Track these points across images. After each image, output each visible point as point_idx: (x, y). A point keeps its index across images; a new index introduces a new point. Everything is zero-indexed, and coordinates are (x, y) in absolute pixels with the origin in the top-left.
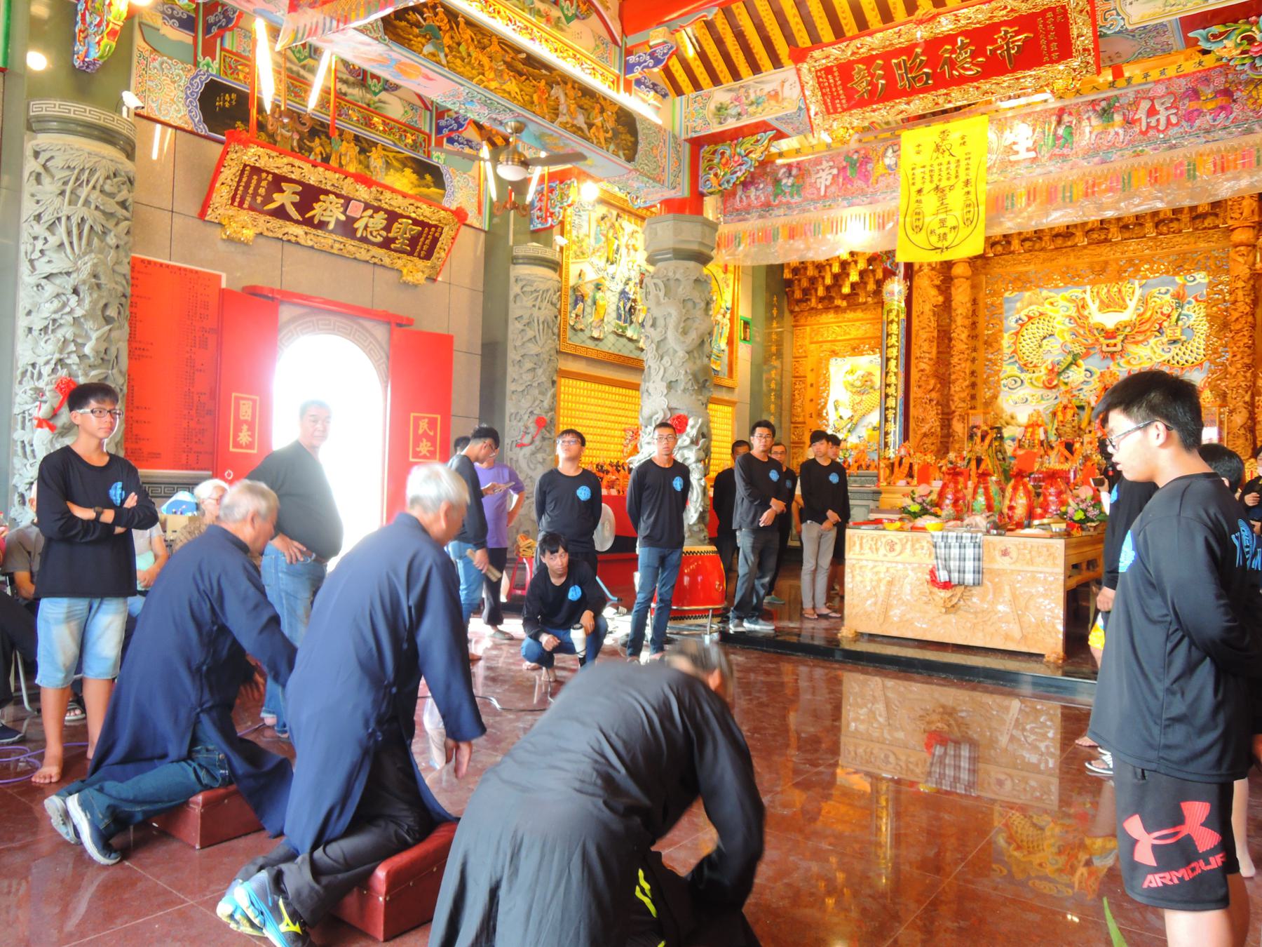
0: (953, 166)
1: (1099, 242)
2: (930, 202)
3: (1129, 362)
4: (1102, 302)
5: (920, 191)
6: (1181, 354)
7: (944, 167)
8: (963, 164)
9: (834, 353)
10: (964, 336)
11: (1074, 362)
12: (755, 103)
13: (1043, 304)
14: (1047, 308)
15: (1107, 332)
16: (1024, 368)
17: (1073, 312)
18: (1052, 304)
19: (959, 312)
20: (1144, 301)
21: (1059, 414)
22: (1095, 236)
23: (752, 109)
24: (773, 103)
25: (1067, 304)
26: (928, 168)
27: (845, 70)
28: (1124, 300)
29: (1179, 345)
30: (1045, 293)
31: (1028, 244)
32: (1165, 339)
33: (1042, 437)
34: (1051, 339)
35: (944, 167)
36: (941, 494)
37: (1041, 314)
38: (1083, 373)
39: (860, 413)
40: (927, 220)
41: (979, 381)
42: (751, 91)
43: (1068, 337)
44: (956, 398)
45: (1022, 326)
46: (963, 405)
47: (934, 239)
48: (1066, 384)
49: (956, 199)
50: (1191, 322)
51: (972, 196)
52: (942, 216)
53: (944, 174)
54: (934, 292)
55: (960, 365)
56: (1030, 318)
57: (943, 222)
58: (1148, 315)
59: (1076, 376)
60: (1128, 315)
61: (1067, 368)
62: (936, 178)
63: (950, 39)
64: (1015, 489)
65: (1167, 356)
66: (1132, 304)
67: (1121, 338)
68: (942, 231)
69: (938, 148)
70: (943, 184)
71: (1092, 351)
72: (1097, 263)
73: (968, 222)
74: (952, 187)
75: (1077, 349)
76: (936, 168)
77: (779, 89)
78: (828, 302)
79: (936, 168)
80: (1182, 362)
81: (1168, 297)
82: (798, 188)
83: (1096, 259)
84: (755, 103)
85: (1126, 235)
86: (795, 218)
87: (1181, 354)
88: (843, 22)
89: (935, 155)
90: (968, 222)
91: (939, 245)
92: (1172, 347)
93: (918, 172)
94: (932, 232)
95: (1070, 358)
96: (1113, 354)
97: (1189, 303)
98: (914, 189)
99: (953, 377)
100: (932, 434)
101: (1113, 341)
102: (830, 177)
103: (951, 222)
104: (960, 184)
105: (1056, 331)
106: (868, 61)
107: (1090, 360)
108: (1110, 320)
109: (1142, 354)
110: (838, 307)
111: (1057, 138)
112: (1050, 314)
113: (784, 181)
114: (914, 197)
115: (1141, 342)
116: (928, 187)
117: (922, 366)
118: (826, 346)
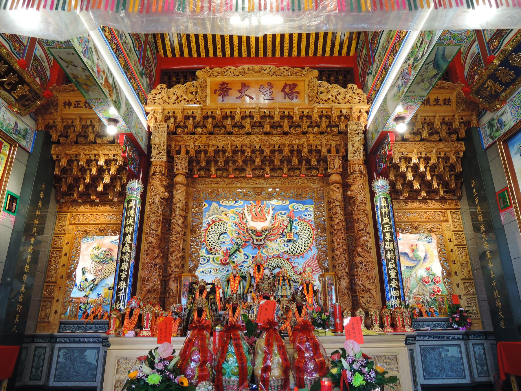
1: (259, 177)
4: (253, 216)
6: (293, 248)
9: (86, 233)
10: (180, 222)
11: (238, 250)
13: (221, 215)
14: (223, 217)
15: (257, 232)
16: (209, 251)
17: (237, 220)
18: (226, 214)
19: (178, 205)
20: (274, 218)
21: (231, 280)
22: (257, 172)
28: (264, 216)
29: (292, 243)
31: (219, 172)
32: (286, 239)
33: (221, 295)
34: (225, 235)
36: (185, 355)
37: (220, 220)
38: (243, 256)
39: (100, 277)
41: (187, 256)
43: (235, 235)
44: (172, 265)
45: (209, 226)
46: (177, 270)
48: (234, 262)
50: (297, 231)
54: (162, 189)
55: (176, 240)
56: (214, 222)
58: (276, 225)
59: (240, 257)
60: (267, 224)
61: (235, 252)
64: (269, 345)
65: (287, 249)
66: (269, 218)
67: (264, 236)
71: (248, 244)
72: (258, 188)
75: (239, 242)
78: (86, 198)
80: (294, 252)
81: (285, 216)
83: (256, 186)
85: (273, 174)
87: (293, 248)
92: (289, 244)
96: (259, 245)
97: (296, 220)
99: (171, 250)
100: (155, 290)
101: (260, 238)
105: (228, 231)
107: (246, 249)
108: (259, 226)
109: (274, 247)
110: (93, 201)
112: (225, 220)
115: (273, 240)
117: (150, 239)
118: (82, 227)
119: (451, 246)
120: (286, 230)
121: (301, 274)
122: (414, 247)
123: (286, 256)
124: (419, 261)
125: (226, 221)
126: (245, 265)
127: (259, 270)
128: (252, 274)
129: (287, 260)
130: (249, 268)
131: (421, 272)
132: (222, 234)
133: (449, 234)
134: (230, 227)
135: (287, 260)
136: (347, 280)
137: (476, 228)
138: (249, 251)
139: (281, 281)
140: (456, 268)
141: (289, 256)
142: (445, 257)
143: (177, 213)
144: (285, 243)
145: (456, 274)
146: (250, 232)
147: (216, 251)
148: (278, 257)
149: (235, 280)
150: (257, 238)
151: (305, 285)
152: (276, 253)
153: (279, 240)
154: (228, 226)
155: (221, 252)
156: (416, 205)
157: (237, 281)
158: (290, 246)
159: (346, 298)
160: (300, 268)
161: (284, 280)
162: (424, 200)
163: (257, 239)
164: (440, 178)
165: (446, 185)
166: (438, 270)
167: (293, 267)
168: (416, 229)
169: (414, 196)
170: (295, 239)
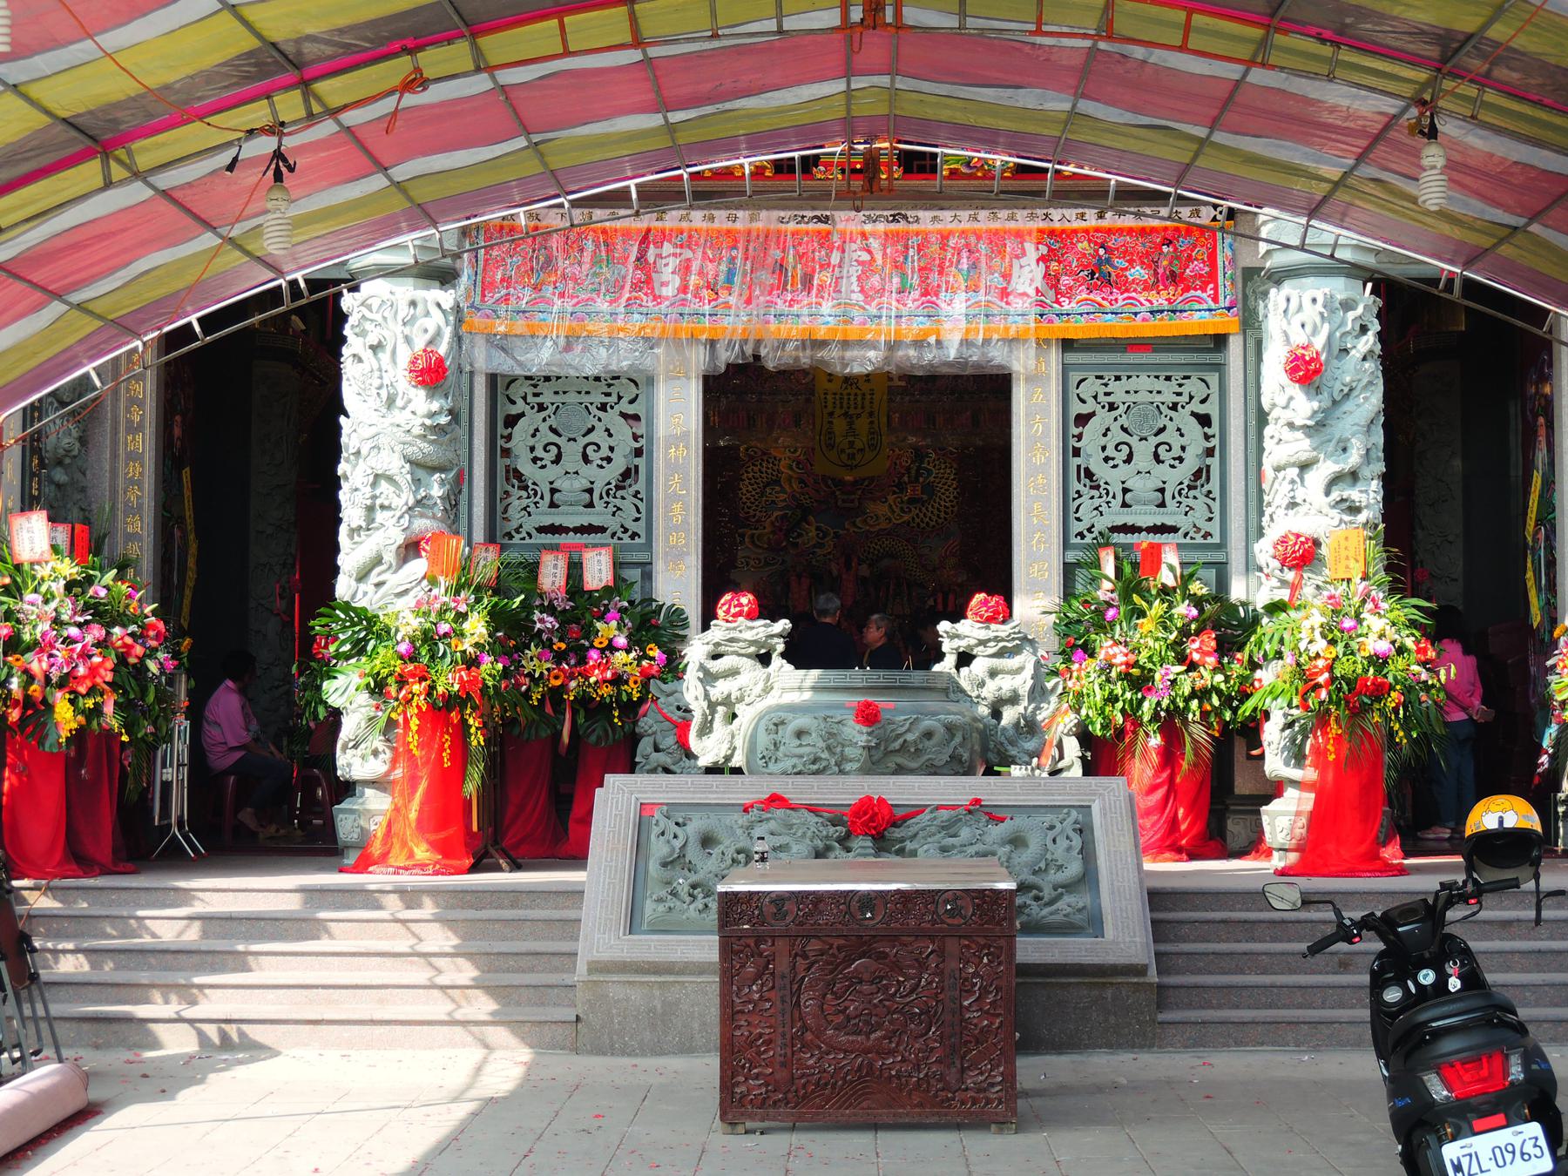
2: (840, 425)
3: (865, 521)
5: (831, 414)
47: (844, 457)
49: (862, 424)
65: (906, 518)
70: (852, 411)
73: (872, 447)
74: (859, 416)
90: (872, 447)
94: (843, 451)
98: (826, 411)
103: (859, 444)
116: (838, 412)
120: (906, 479)
125: (779, 456)
128: (835, 573)
132: (768, 484)
151: (940, 595)
170: (925, 497)
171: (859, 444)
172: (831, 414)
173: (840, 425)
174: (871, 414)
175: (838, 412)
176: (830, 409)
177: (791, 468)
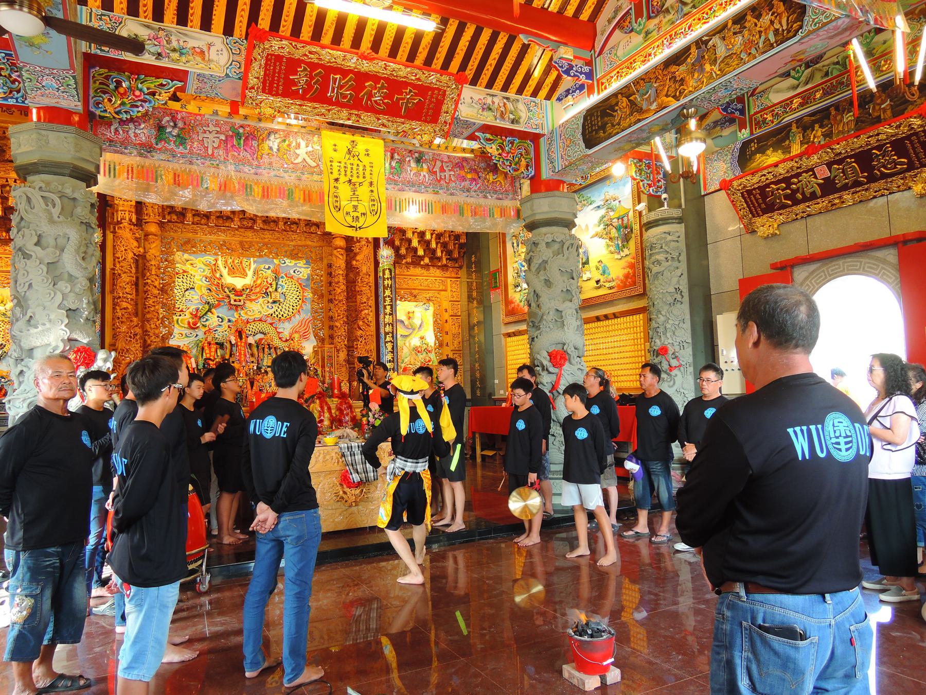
0: (361, 168)
1: (247, 228)
2: (344, 191)
5: (337, 180)
7: (355, 167)
8: (368, 168)
12: (180, 51)
13: (185, 265)
14: (188, 267)
17: (208, 273)
19: (153, 263)
20: (256, 273)
22: (245, 223)
23: (175, 56)
24: (199, 59)
25: (204, 267)
26: (342, 165)
27: (293, 64)
30: (186, 256)
31: (196, 219)
32: (271, 301)
34: (192, 292)
35: (355, 167)
37: (184, 271)
40: (343, 203)
42: (173, 38)
43: (205, 291)
47: (349, 219)
51: (375, 194)
52: (356, 203)
53: (355, 172)
57: (355, 207)
58: (259, 282)
59: (212, 320)
60: (248, 281)
62: (348, 173)
63: (375, 78)
65: (271, 311)
66: (250, 273)
68: (355, 214)
69: (349, 152)
70: (354, 180)
75: (211, 301)
76: (349, 166)
77: (205, 49)
79: (349, 166)
81: (269, 271)
82: (182, 140)
84: (180, 51)
85: (265, 227)
86: (178, 165)
88: (283, 23)
89: (348, 156)
91: (354, 224)
93: (335, 164)
95: (207, 307)
96: (237, 306)
102: (217, 141)
103: (361, 209)
104: (366, 184)
105: (196, 286)
106: (313, 66)
107: (220, 310)
109: (255, 309)
111: (392, 168)
113: (169, 130)
114: (333, 184)
115: (254, 300)
117: (124, 305)
119: (446, 316)
120: (270, 289)
121: (287, 340)
122: (411, 315)
123: (270, 320)
124: (414, 330)
126: (220, 329)
127: (241, 338)
128: (233, 342)
129: (271, 324)
130: (223, 333)
131: (415, 341)
133: (446, 304)
134: (200, 282)
135: (271, 324)
136: (345, 352)
137: (470, 299)
138: (223, 311)
139: (266, 350)
140: (447, 339)
141: (274, 321)
142: (439, 327)
143: (153, 273)
144: (270, 305)
145: (447, 345)
146: (226, 290)
147: (182, 311)
148: (260, 320)
149: (210, 349)
150: (237, 298)
152: (258, 316)
153: (261, 300)
154: (196, 281)
155: (187, 313)
156: (418, 271)
157: (213, 350)
158: (275, 309)
159: (344, 369)
160: (286, 335)
161: (270, 348)
162: (426, 267)
163: (236, 299)
164: (445, 245)
165: (449, 253)
166: (431, 340)
167: (279, 333)
168: (415, 298)
169: (416, 261)
170: (282, 300)
171: (361, 209)
172: (337, 180)
173: (344, 191)
174: (371, 184)
175: (343, 179)
176: (335, 175)
177: (201, 280)
